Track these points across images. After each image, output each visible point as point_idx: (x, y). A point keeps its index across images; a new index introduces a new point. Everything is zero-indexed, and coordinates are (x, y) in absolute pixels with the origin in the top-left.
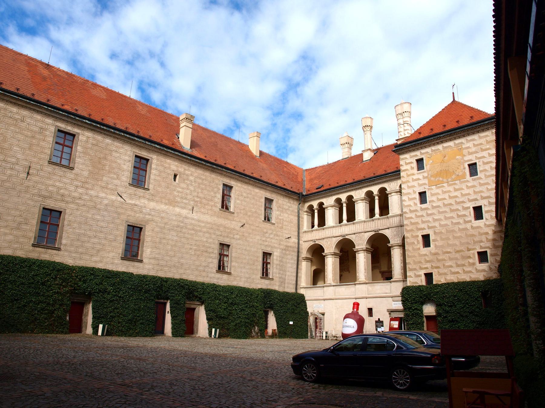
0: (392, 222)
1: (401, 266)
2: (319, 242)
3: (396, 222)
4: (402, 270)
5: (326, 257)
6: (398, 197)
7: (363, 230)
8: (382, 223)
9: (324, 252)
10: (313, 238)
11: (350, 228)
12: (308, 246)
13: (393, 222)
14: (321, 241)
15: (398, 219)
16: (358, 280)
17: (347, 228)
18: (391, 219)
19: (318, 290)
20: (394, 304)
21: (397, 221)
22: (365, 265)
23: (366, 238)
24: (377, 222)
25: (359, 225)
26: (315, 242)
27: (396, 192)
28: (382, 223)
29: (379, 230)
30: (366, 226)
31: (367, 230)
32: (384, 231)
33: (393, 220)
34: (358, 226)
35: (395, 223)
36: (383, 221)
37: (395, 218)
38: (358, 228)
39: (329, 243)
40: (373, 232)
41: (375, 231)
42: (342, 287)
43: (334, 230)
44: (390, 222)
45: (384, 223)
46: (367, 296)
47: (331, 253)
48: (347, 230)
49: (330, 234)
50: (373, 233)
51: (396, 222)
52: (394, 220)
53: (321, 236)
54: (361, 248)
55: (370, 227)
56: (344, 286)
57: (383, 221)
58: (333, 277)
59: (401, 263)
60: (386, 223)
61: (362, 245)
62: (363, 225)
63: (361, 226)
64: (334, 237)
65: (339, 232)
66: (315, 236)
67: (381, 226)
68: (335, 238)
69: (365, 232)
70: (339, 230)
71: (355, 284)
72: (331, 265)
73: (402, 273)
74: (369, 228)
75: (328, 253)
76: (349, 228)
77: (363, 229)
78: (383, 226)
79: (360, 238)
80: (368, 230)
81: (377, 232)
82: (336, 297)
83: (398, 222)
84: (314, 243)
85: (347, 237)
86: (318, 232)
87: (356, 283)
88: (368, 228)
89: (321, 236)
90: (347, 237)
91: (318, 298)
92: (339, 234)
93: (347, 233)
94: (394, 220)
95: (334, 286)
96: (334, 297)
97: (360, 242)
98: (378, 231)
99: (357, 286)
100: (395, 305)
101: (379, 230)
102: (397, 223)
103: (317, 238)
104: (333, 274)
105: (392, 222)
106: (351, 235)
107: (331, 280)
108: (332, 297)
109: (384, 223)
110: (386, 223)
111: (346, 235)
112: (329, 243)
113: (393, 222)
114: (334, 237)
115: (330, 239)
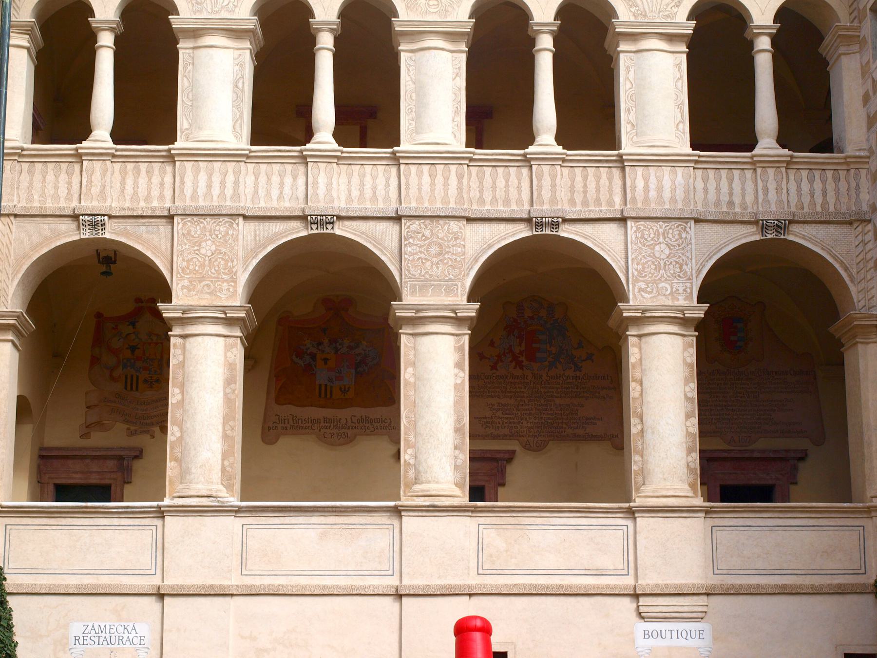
0: (646, 189)
1: (688, 434)
2: (126, 234)
3: (667, 195)
4: (689, 451)
5: (176, 331)
6: (678, 66)
7: (452, 207)
8: (579, 186)
9: (169, 300)
10: (89, 205)
11: (368, 179)
12: (34, 248)
13: (653, 194)
14: (141, 230)
15: (680, 179)
16: (409, 486)
17: (343, 180)
18: (640, 170)
19: (108, 534)
20: (647, 635)
21: (674, 190)
22: (457, 403)
23: (471, 252)
24: (553, 178)
25: (432, 176)
26: (94, 225)
27: (670, 38)
28: (579, 186)
29: (565, 220)
30: (475, 184)
31: (476, 210)
32: (588, 228)
33: (653, 181)
34: (426, 179)
35: (660, 196)
36: (585, 178)
37: (666, 170)
38: (426, 187)
39: (208, 248)
40: (522, 226)
41: (540, 225)
42: (301, 520)
43: (250, 179)
44: (634, 188)
45: (592, 186)
46: (473, 581)
47: (224, 309)
48: (343, 187)
49: (222, 195)
50: (522, 232)
51: (667, 195)
52: (660, 181)
53: (148, 198)
54: (446, 307)
55: (500, 194)
56: (315, 519)
57: (585, 178)
58: (225, 456)
59: (688, 416)
60: (604, 191)
61: (450, 290)
62: (460, 177)
63: (447, 179)
64: (245, 217)
65: (287, 190)
66: (95, 190)
67: (572, 202)
68: (252, 225)
69: (469, 220)
70: (288, 180)
71: (160, 513)
72: (220, 383)
73: (691, 470)
74: (494, 200)
75: (205, 308)
76: (355, 180)
77: (460, 198)
78: (585, 203)
79: (434, 250)
80: (487, 209)
81: (547, 231)
82: (249, 581)
83: (680, 194)
84: (86, 234)
85: (338, 231)
86: (124, 173)
87: (405, 501)
88: (488, 196)
89: (148, 198)
90: (340, 230)
91: (105, 580)
92: (287, 204)
93: (340, 205)
94: (660, 181)
95: (238, 511)
96: (234, 580)
97: (438, 271)
98: (555, 225)
99: (410, 522)
100: (651, 642)
101: (565, 220)
102: (673, 200)
103: (113, 204)
104: (225, 437)
105: (646, 189)
106: (371, 224)
107: (216, 475)
108: (226, 583)
109: (592, 186)
110: (604, 191)
111: (340, 218)
112: (208, 248)
113: (653, 194)
114: (245, 217)
115: (221, 227)
